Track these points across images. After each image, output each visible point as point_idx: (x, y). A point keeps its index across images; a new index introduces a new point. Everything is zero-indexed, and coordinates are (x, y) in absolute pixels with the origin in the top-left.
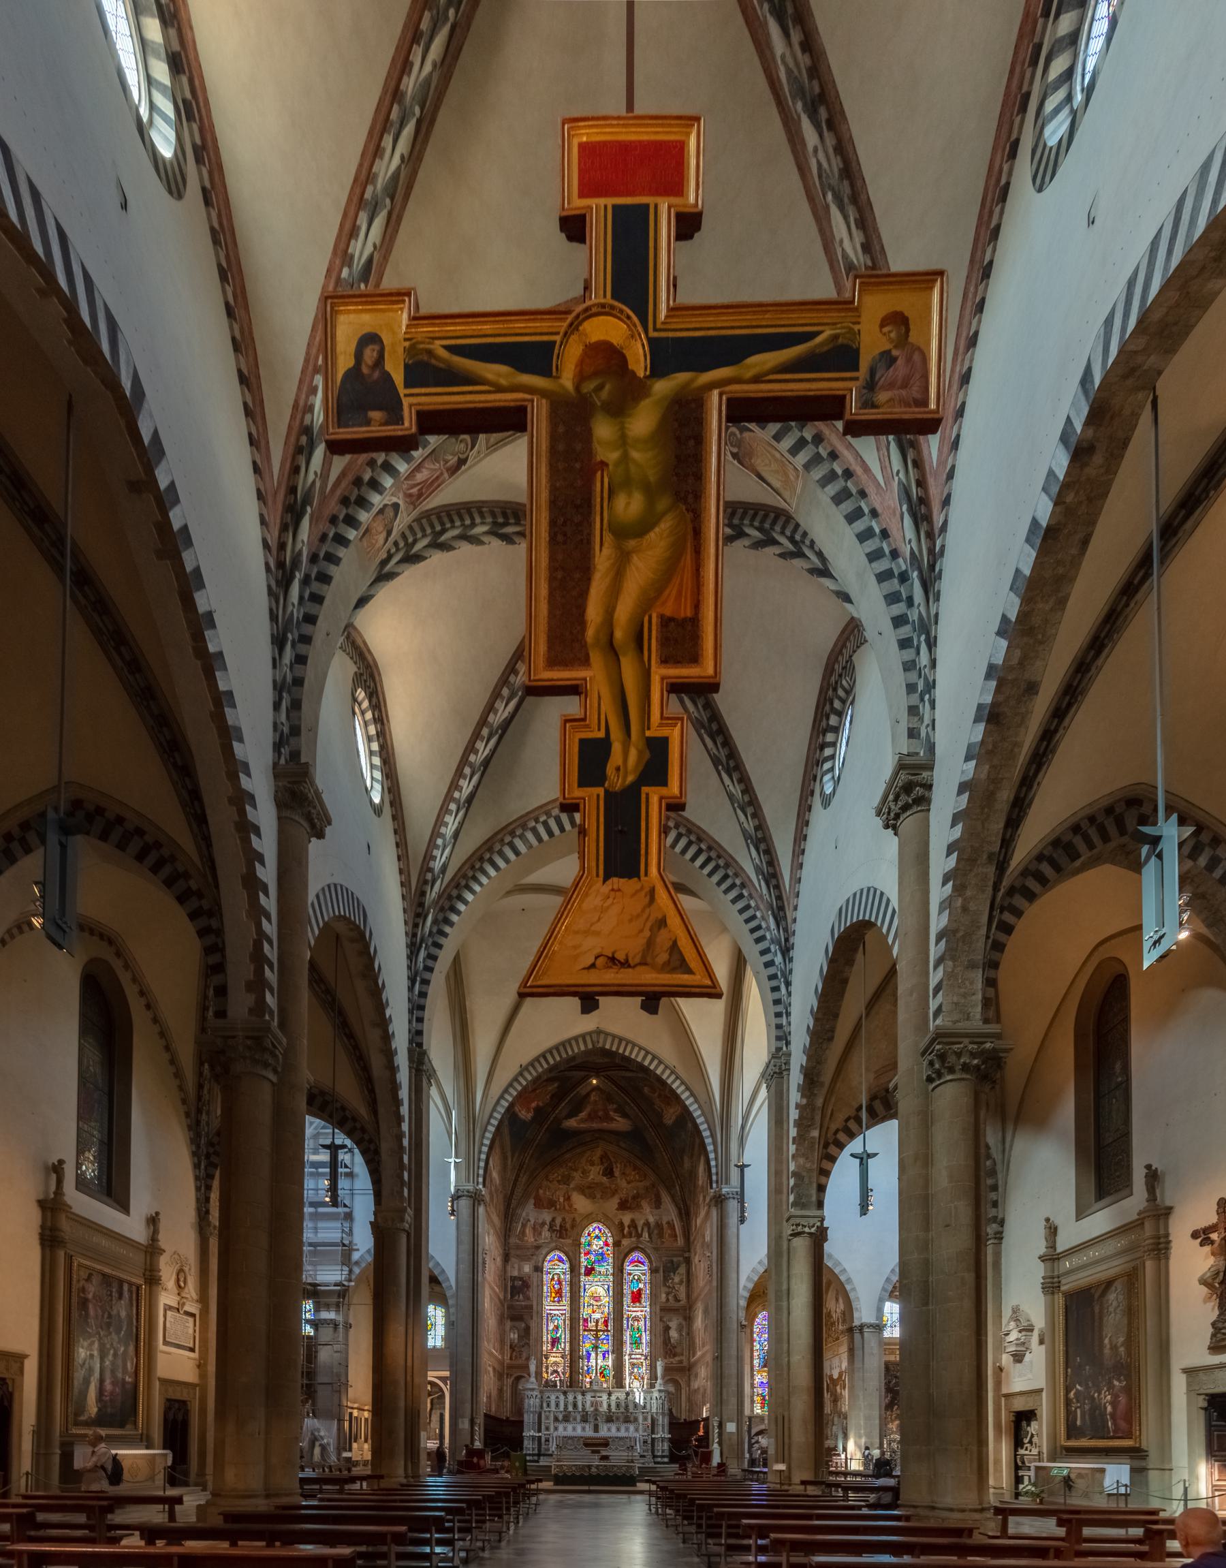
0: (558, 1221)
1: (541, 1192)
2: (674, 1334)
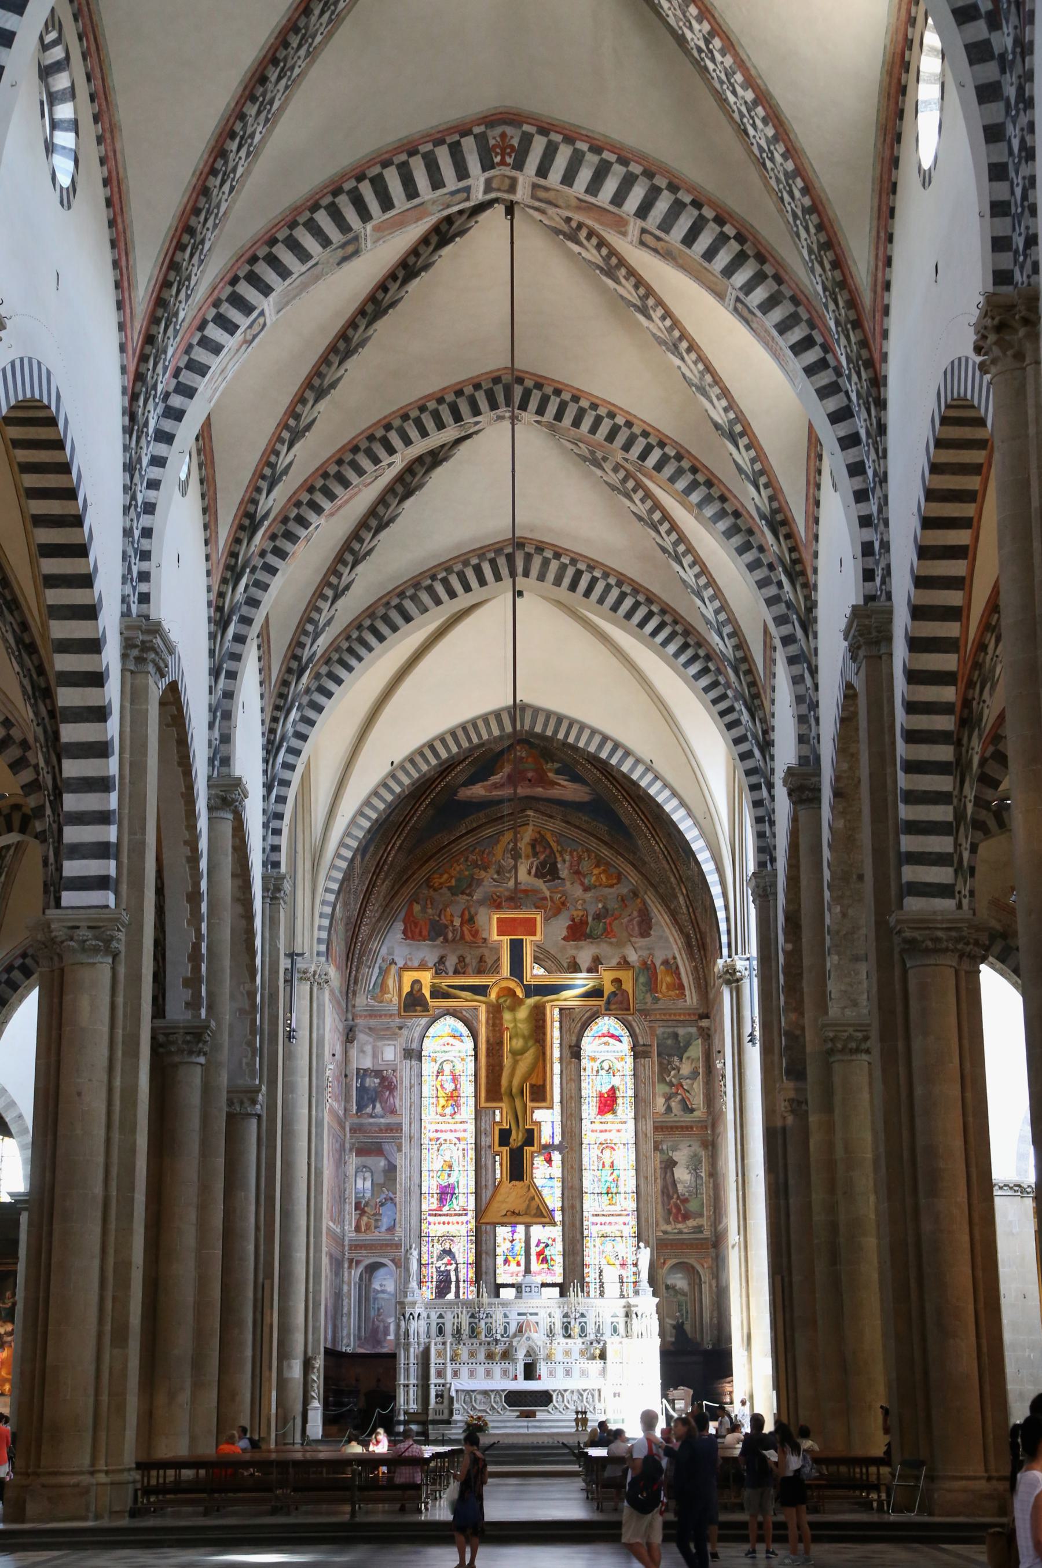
1: (417, 908)
2: (682, 1175)
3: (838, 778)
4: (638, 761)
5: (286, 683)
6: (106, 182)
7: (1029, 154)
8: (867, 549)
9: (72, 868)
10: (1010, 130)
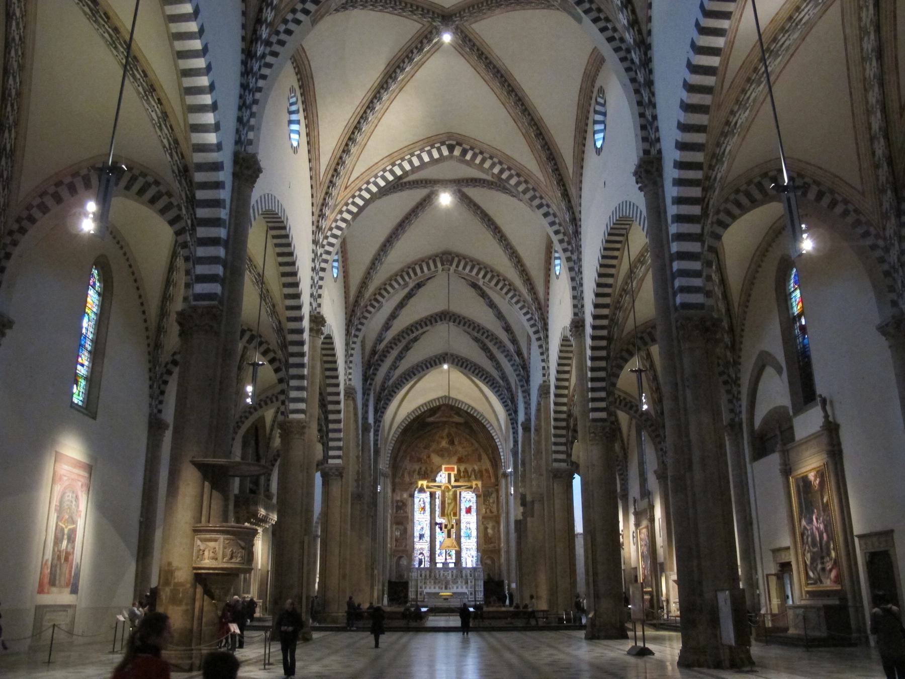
0: (423, 469)
2: (490, 531)
3: (536, 426)
4: (479, 413)
5: (380, 393)
6: (344, 272)
7: (581, 285)
8: (544, 368)
9: (331, 453)
10: (577, 279)
